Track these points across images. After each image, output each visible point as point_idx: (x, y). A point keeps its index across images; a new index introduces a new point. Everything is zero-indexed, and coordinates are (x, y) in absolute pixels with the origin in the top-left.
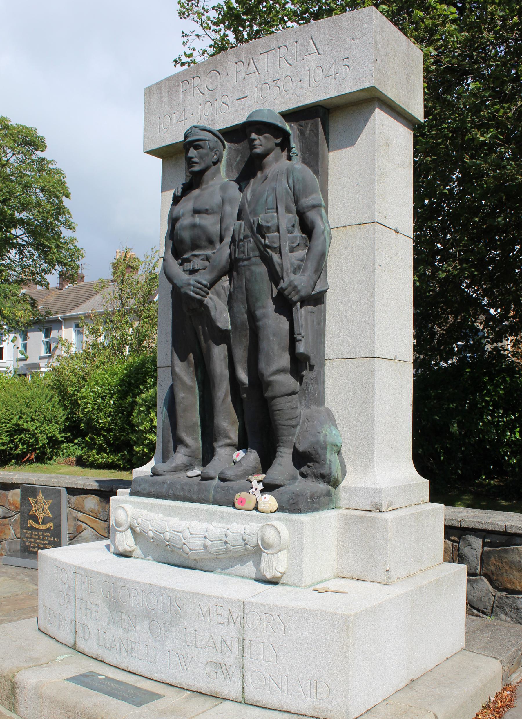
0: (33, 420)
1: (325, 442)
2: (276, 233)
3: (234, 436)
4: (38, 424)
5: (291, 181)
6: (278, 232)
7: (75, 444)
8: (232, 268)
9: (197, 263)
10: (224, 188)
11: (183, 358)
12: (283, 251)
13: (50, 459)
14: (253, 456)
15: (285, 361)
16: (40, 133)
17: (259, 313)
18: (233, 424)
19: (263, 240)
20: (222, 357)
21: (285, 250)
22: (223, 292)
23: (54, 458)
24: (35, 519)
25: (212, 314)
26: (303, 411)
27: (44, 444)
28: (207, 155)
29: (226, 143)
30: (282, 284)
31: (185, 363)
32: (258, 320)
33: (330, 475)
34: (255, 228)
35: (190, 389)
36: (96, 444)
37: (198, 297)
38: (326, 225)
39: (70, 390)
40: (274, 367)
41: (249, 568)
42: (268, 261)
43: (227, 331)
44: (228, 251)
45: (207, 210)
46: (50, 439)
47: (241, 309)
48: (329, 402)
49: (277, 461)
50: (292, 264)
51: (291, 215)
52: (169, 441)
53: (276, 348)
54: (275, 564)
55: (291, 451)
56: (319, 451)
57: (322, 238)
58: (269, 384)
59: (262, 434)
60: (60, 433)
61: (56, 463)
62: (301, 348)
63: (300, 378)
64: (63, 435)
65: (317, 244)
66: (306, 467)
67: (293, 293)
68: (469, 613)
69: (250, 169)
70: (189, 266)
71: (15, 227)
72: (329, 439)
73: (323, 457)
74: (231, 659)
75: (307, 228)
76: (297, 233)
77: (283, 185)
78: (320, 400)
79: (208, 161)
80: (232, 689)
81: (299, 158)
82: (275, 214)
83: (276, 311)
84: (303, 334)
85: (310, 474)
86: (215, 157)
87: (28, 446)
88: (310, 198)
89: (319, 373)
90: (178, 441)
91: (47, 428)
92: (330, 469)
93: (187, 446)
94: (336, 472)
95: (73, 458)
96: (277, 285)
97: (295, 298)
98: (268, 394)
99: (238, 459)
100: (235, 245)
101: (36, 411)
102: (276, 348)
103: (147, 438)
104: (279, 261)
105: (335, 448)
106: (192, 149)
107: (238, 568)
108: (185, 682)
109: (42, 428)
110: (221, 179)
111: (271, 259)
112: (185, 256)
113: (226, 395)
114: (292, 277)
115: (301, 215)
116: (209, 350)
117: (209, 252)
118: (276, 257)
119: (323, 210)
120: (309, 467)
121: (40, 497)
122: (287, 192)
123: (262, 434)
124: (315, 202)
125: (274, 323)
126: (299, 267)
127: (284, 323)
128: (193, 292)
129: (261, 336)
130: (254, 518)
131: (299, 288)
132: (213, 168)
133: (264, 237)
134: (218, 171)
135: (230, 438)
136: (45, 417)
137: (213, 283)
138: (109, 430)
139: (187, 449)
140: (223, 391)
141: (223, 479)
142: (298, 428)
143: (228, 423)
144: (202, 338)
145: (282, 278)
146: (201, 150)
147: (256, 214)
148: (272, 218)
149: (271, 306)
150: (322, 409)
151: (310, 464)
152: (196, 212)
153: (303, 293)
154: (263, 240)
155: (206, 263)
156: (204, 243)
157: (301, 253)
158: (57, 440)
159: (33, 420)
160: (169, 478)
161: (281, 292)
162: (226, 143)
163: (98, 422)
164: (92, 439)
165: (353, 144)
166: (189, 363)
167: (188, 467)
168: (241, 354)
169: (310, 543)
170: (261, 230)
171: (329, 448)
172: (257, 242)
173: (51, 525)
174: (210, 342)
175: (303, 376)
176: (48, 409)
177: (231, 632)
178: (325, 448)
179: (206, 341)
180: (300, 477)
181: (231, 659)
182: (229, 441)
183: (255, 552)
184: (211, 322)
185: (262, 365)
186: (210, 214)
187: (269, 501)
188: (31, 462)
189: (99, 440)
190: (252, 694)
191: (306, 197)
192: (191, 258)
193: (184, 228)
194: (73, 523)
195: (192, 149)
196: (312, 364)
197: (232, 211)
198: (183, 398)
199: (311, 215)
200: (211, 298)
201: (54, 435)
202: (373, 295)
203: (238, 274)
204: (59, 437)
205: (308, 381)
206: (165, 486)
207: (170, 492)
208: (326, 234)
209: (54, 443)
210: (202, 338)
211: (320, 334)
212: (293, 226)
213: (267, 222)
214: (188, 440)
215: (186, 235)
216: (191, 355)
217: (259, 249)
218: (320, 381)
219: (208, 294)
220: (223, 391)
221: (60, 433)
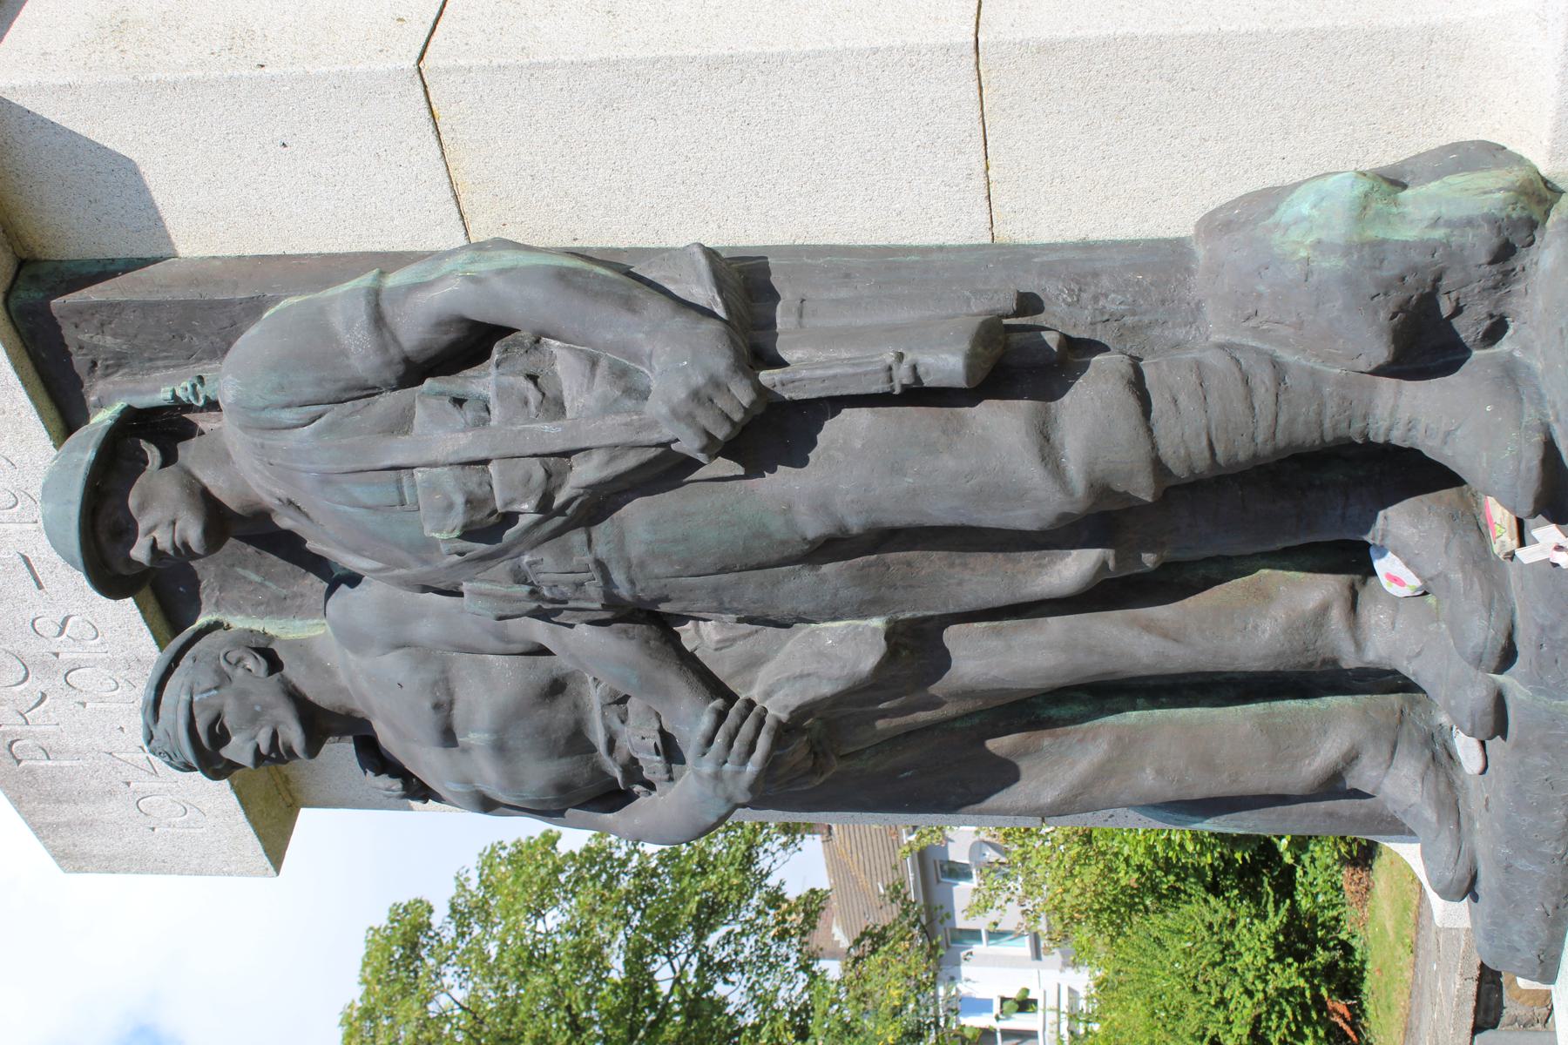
0: (1222, 1003)
1: (1347, 250)
2: (491, 468)
3: (1316, 590)
4: (1234, 989)
5: (288, 416)
6: (486, 462)
7: (1297, 859)
8: (651, 620)
9: (638, 739)
10: (354, 640)
11: (1005, 773)
12: (559, 446)
13: (1348, 949)
15: (1001, 423)
16: (381, 920)
17: (813, 528)
18: (1265, 596)
19: (524, 521)
20: (995, 644)
21: (552, 434)
22: (740, 647)
23: (1343, 936)
25: (826, 689)
26: (1216, 328)
27: (1301, 974)
28: (242, 696)
29: (202, 620)
30: (689, 445)
31: (1023, 765)
32: (843, 529)
33: (1495, 223)
34: (481, 548)
35: (1125, 745)
37: (763, 743)
38: (447, 266)
39: (1128, 878)
40: (1031, 471)
42: (601, 503)
43: (891, 634)
44: (583, 630)
45: (437, 707)
46: (1284, 951)
47: (800, 584)
48: (1170, 216)
50: (609, 407)
51: (420, 413)
52: (1331, 815)
53: (949, 462)
55: (1386, 383)
56: (1390, 270)
57: (498, 284)
58: (1101, 491)
60: (1263, 917)
61: (1359, 933)
62: (947, 364)
63: (1079, 350)
64: (1270, 907)
66: (1457, 323)
67: (721, 402)
70: (652, 765)
71: (652, 984)
72: (1338, 230)
73: (1417, 258)
76: (483, 381)
78: (1164, 260)
79: (264, 689)
81: (207, 369)
82: (419, 475)
83: (798, 459)
84: (889, 357)
86: (250, 663)
87: (1308, 1020)
88: (346, 339)
89: (1048, 270)
91: (1247, 958)
92: (1470, 222)
93: (1351, 758)
94: (1482, 194)
95: (1345, 876)
96: (691, 465)
97: (743, 394)
98: (1143, 489)
99: (1413, 582)
100: (558, 612)
101: (1195, 989)
102: (949, 462)
104: (597, 458)
105: (1378, 205)
106: (227, 752)
109: (1250, 976)
111: (593, 489)
112: (617, 774)
113: (1148, 627)
114: (656, 407)
115: (414, 372)
117: (594, 698)
118: (584, 473)
119: (393, 280)
120: (1458, 311)
122: (331, 428)
124: (362, 317)
125: (851, 473)
126: (621, 374)
127: (844, 432)
128: (744, 763)
131: (698, 380)
132: (294, 671)
133: (510, 518)
134: (301, 648)
135: (1324, 609)
136: (1214, 965)
137: (713, 686)
139: (1365, 760)
140: (1130, 639)
141: (1508, 657)
142: (1287, 356)
144: (923, 716)
145: (666, 445)
146: (229, 721)
147: (431, 545)
148: (432, 487)
149: (782, 481)
150: (1201, 252)
151: (1446, 308)
152: (448, 737)
153: (720, 362)
154: (524, 521)
155: (634, 705)
156: (560, 713)
157: (564, 364)
158: (1287, 929)
159: (1222, 1003)
160: (1485, 844)
162: (202, 620)
165: (128, 168)
166: (1026, 753)
168: (984, 579)
170: (487, 528)
171: (1376, 232)
172: (533, 539)
174: (936, 689)
175: (1069, 343)
176: (1187, 954)
178: (1379, 246)
179: (936, 703)
180: (1504, 346)
182: (1337, 615)
184: (859, 697)
185: (1023, 518)
186: (450, 692)
188: (1357, 1013)
191: (344, 353)
192: (621, 756)
195: (227, 752)
196: (1010, 304)
197: (432, 616)
198: (1160, 772)
199: (414, 329)
200: (768, 694)
201: (1273, 937)
202: (714, 65)
203: (666, 599)
204: (1276, 920)
205: (1087, 315)
206: (1521, 863)
207: (1548, 849)
208: (481, 267)
209: (1297, 939)
210: (923, 716)
211: (888, 269)
212: (459, 402)
213: (450, 506)
214: (1327, 753)
215: (539, 773)
216: (992, 744)
217: (557, 533)
218: (1083, 262)
219: (750, 704)
220: (1130, 639)
221: (1263, 917)
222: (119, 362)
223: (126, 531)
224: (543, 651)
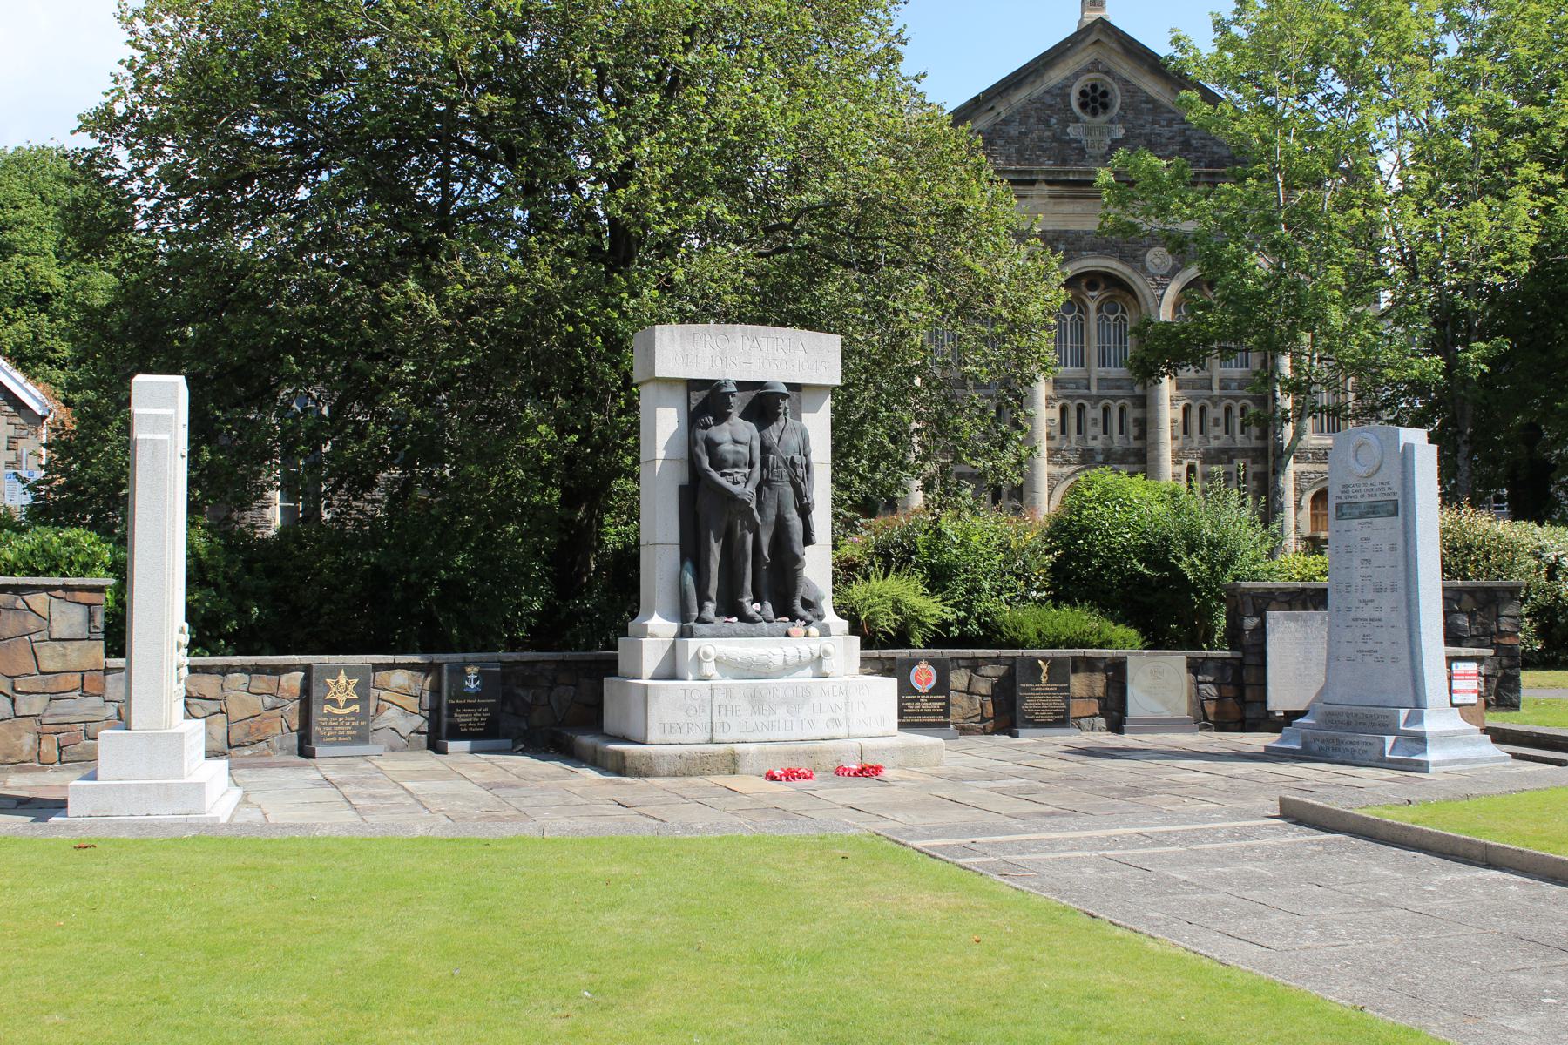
9: (739, 477)
14: (768, 606)
24: (334, 702)
41: (809, 671)
54: (826, 668)
74: (841, 715)
75: (808, 468)
80: (842, 732)
107: (801, 673)
116: (744, 537)
121: (343, 679)
168: (765, 540)
173: (357, 707)
177: (841, 700)
190: (853, 733)
197: (756, 444)
215: (730, 458)
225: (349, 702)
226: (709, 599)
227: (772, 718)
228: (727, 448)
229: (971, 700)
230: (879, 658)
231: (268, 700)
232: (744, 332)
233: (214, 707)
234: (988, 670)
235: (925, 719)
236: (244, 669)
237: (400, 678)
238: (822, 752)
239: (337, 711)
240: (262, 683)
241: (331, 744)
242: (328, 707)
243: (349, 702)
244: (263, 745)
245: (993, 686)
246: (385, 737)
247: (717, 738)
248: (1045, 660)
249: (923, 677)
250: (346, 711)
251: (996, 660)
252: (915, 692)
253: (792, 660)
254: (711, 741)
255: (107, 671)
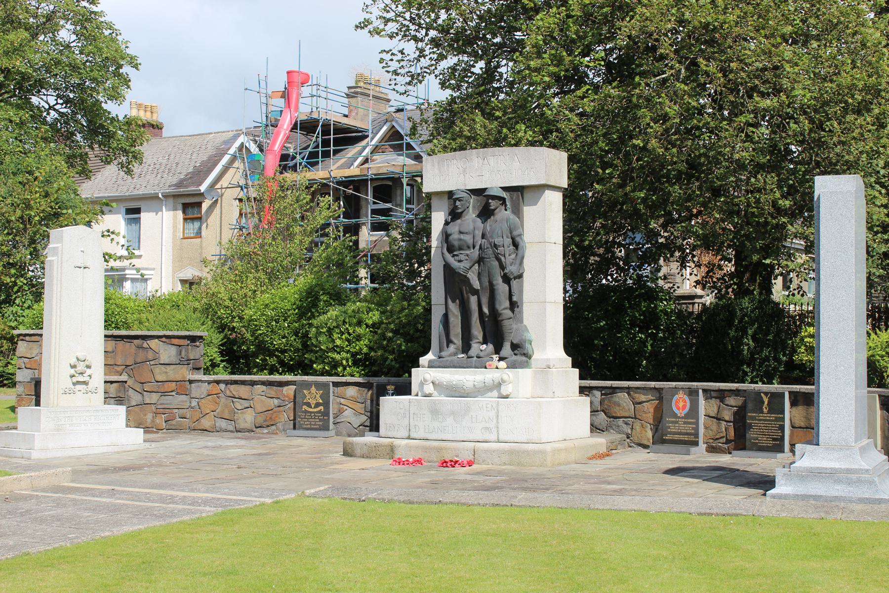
8: (480, 260)
9: (462, 257)
10: (474, 221)
11: (453, 301)
14: (491, 347)
15: (507, 304)
17: (494, 282)
21: (507, 255)
24: (309, 405)
26: (514, 326)
36: (267, 364)
40: (503, 307)
41: (495, 393)
48: (525, 322)
49: (504, 348)
58: (500, 314)
59: (495, 335)
63: (513, 311)
65: (520, 252)
68: (592, 431)
69: (486, 213)
74: (492, 425)
75: (516, 245)
76: (512, 247)
77: (505, 226)
78: (522, 322)
80: (493, 437)
85: (520, 352)
90: (449, 342)
94: (530, 352)
98: (500, 319)
103: (328, 357)
107: (490, 394)
108: (471, 438)
110: (471, 217)
115: (513, 239)
117: (468, 252)
118: (503, 258)
121: (313, 389)
123: (495, 335)
125: (502, 288)
129: (496, 292)
130: (496, 371)
138: (283, 352)
141: (478, 357)
143: (477, 331)
149: (500, 280)
152: (461, 232)
156: (465, 247)
157: (513, 256)
161: (505, 275)
163: (272, 343)
164: (264, 360)
167: (455, 354)
169: (520, 381)
172: (494, 252)
173: (322, 408)
177: (492, 414)
181: (492, 425)
183: (498, 385)
187: (503, 364)
189: (272, 361)
190: (502, 438)
193: (455, 240)
194: (336, 406)
197: (479, 234)
199: (517, 239)
214: (455, 341)
215: (456, 243)
218: (521, 312)
222: (512, 198)
223: (493, 199)
224: (474, 248)
225: (317, 405)
226: (452, 342)
227: (444, 424)
228: (455, 237)
229: (719, 425)
230: (655, 388)
231: (276, 401)
232: (478, 154)
233: (246, 404)
234: (732, 401)
235: (682, 437)
236: (263, 383)
237: (352, 391)
238: (446, 449)
239: (310, 410)
240: (272, 391)
241: (307, 429)
242: (305, 407)
243: (317, 405)
244: (274, 427)
245: (735, 414)
246: (343, 428)
247: (412, 436)
248: (766, 394)
249: (681, 404)
250: (316, 410)
251: (737, 393)
252: (675, 415)
253: (479, 385)
254: (409, 438)
255: (191, 382)
